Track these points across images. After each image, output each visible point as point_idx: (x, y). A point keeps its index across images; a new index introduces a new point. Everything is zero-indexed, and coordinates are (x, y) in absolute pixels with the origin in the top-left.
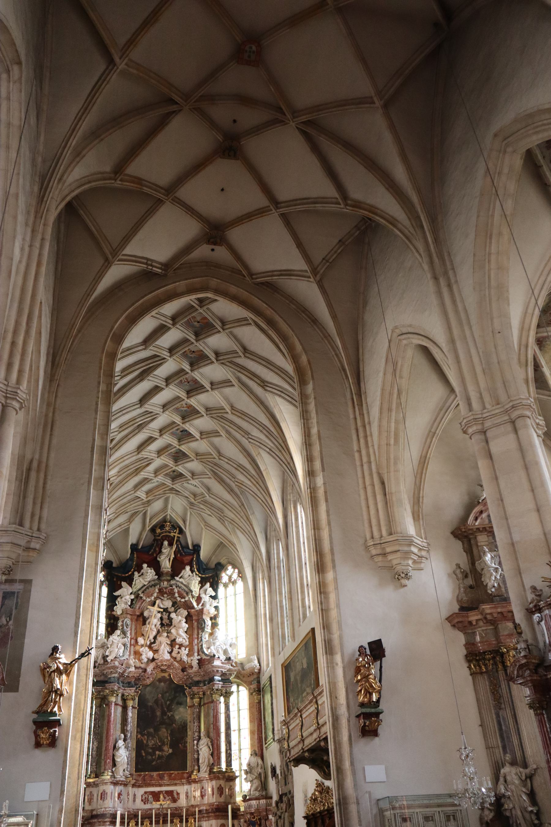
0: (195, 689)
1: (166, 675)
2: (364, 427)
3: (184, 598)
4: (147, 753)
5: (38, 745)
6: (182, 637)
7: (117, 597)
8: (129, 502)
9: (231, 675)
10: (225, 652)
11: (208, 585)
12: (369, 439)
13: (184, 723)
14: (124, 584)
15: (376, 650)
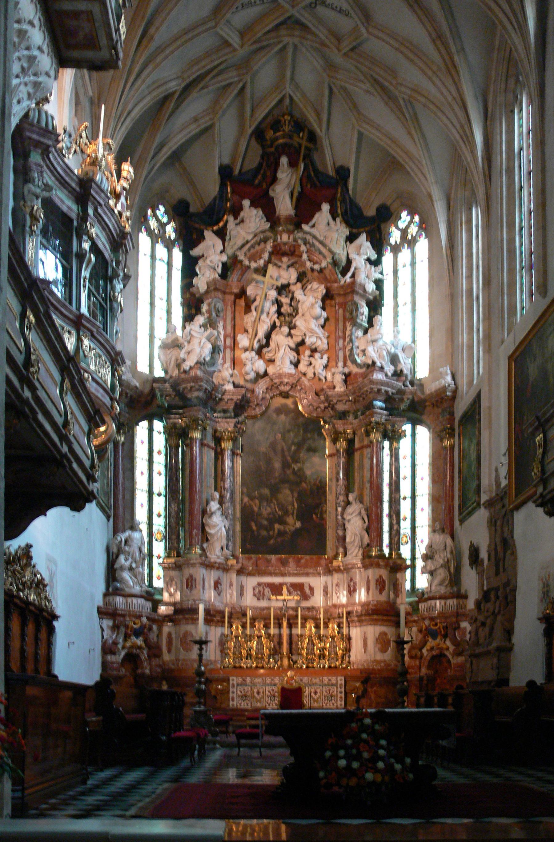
0: (340, 425)
4: (260, 526)
13: (320, 482)
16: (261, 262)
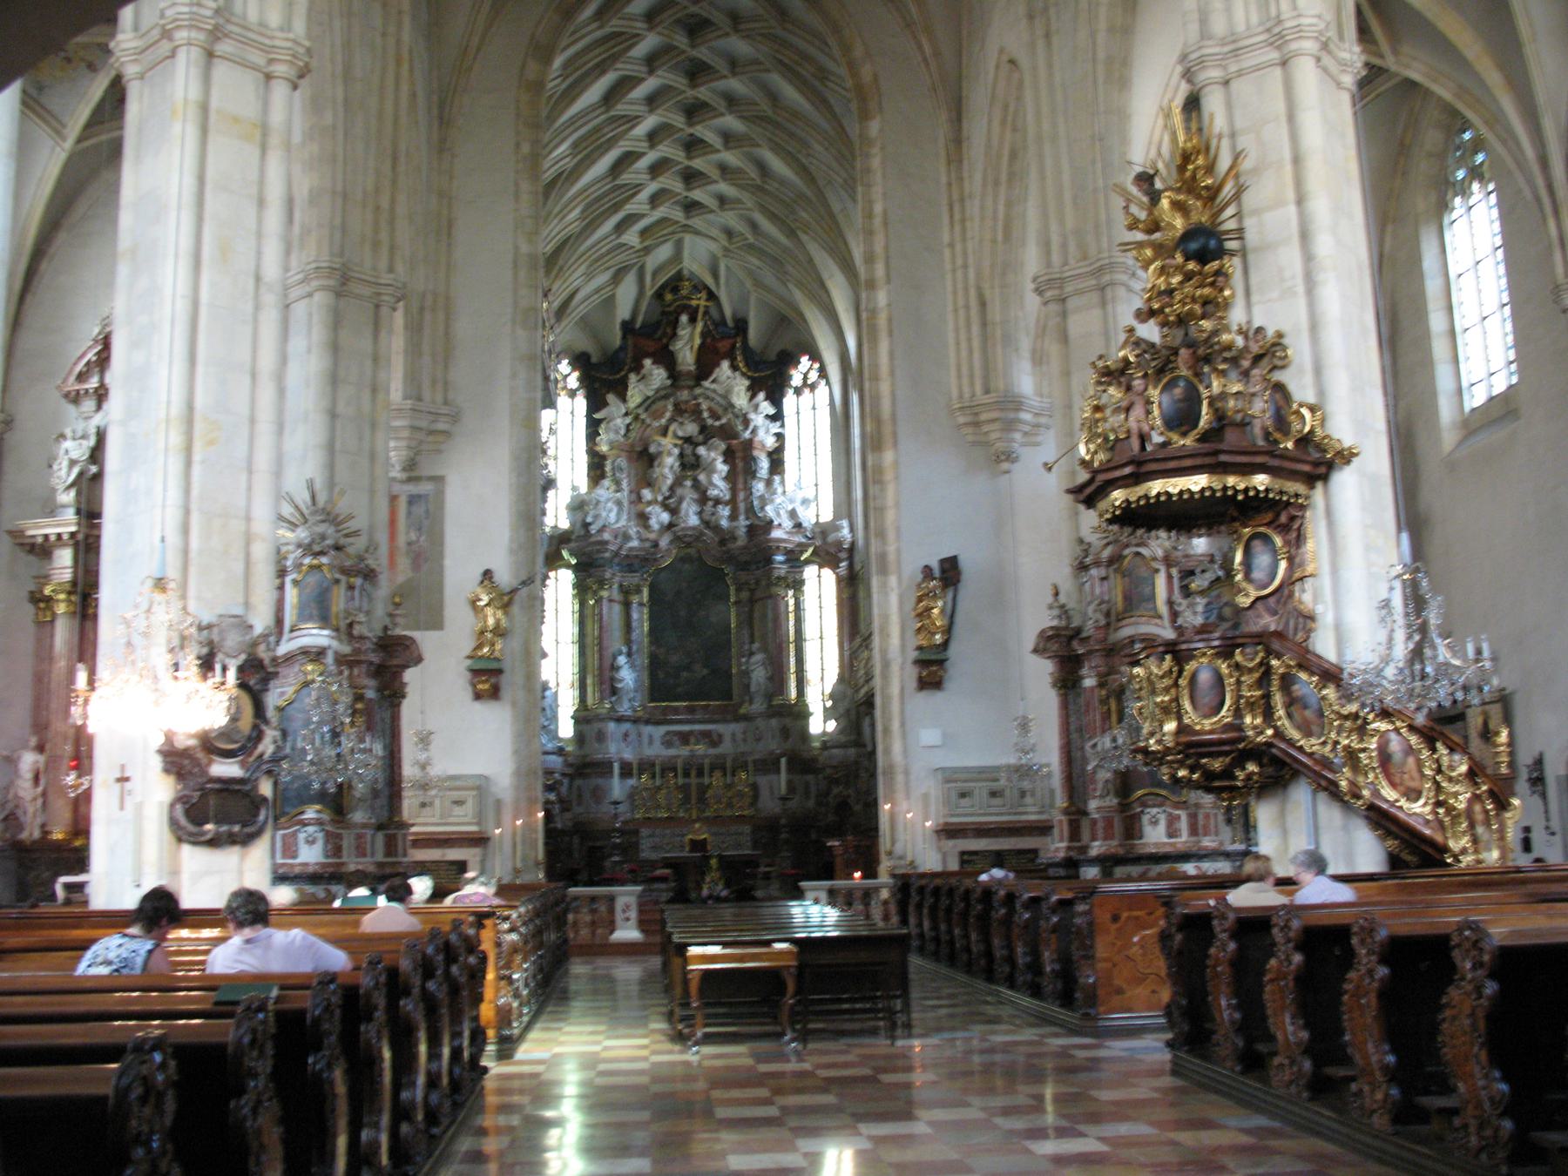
0: (743, 576)
1: (692, 551)
2: (962, 200)
3: (718, 418)
5: (478, 696)
6: (719, 485)
7: (600, 421)
8: (609, 252)
9: (802, 553)
10: (793, 514)
11: (761, 396)
12: (968, 224)
14: (611, 398)
15: (949, 573)
16: (663, 421)
